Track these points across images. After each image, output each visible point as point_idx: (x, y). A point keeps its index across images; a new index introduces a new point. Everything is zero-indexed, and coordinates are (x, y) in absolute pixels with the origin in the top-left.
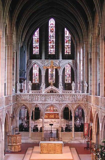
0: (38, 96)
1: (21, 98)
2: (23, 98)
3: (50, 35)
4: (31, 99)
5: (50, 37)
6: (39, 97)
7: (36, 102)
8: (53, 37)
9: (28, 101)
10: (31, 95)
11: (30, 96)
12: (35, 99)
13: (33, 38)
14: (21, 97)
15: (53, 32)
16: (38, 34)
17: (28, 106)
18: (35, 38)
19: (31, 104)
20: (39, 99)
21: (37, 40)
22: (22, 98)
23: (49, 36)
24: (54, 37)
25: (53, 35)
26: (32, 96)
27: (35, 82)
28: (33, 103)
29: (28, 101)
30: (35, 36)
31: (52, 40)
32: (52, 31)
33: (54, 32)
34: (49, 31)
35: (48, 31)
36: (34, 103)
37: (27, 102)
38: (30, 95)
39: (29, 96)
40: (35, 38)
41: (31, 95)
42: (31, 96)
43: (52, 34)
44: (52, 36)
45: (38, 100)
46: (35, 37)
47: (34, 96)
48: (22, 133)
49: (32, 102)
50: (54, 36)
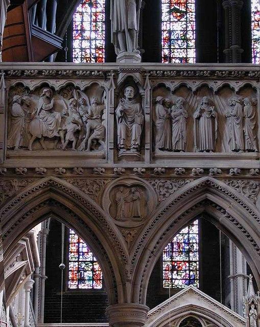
0: (217, 100)
1: (21, 122)
2: (45, 124)
3: (170, 32)
4: (135, 129)
5: (169, 40)
6: (227, 106)
7: (196, 165)
8: (186, 40)
9: (106, 147)
10: (136, 86)
11: (129, 91)
12: (178, 128)
13: (72, 21)
14: (16, 108)
15: (183, 14)
16: (100, 24)
17: (107, 201)
18: (82, 49)
19: (130, 186)
20: (232, 130)
21: (96, 58)
22: (31, 118)
23: (165, 35)
24: (192, 43)
25: (185, 31)
26: (146, 93)
27: (81, 286)
28: (160, 165)
29: (106, 147)
30: (83, 39)
31: (181, 59)
32: (177, 11)
33: (192, 16)
34: (165, 8)
35: (159, 13)
36: (180, 165)
37: (103, 158)
38: (129, 81)
39: (119, 95)
40: (82, 49)
41: (136, 86)
42: (138, 98)
43: (178, 27)
44: (177, 39)
45: (217, 141)
46: (85, 44)
47: (177, 99)
48: (119, 302)
49: (154, 158)
50: (190, 35)
